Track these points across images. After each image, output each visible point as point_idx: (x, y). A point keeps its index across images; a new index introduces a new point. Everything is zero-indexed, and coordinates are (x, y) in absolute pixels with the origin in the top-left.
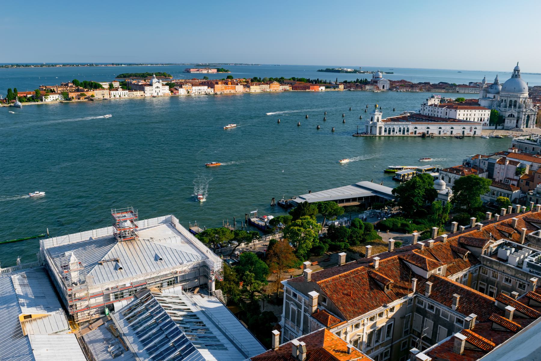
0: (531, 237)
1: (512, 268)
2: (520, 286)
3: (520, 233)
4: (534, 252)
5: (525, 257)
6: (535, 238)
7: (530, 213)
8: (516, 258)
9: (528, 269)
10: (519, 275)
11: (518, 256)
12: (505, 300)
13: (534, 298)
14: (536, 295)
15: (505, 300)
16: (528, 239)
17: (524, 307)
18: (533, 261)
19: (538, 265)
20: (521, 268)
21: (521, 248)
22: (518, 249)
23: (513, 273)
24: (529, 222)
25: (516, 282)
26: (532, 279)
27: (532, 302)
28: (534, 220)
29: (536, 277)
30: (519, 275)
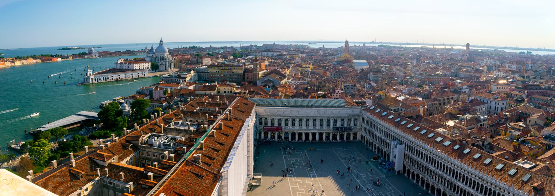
0: (166, 128)
1: (156, 148)
2: (162, 157)
3: (160, 127)
4: (166, 136)
5: (162, 141)
6: (168, 128)
7: (166, 115)
8: (157, 143)
9: (164, 147)
10: (160, 152)
11: (158, 141)
12: (149, 169)
13: (165, 163)
14: (166, 161)
15: (149, 169)
16: (166, 129)
17: (159, 170)
18: (165, 142)
19: (168, 144)
20: (160, 147)
21: (160, 136)
22: (158, 136)
23: (157, 151)
24: (165, 120)
25: (159, 156)
26: (165, 153)
27: (165, 166)
28: (167, 118)
29: (167, 151)
30: (160, 152)
